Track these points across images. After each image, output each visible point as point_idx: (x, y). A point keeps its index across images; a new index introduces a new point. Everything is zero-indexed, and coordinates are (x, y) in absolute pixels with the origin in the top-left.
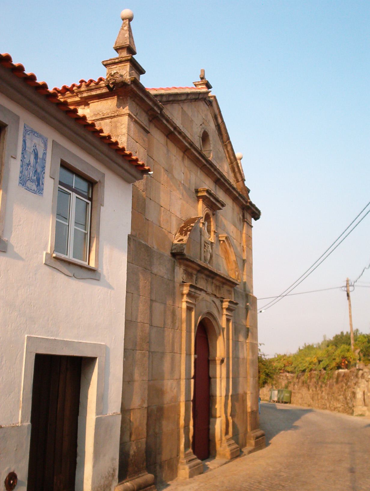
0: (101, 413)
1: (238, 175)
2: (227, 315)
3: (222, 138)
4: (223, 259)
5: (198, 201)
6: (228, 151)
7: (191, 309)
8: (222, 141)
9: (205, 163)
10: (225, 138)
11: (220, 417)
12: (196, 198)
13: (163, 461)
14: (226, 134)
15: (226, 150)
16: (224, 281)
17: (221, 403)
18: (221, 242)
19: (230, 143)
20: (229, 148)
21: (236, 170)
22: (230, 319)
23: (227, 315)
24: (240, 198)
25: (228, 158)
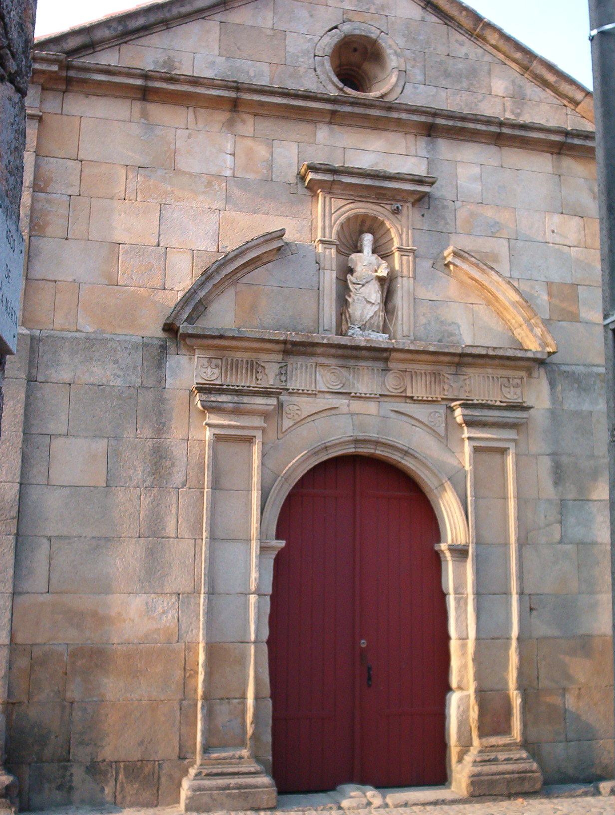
0: (496, 732)
1: (565, 88)
2: (469, 439)
3: (460, 26)
4: (475, 307)
5: (316, 196)
6: (495, 47)
7: (506, 451)
8: (464, 33)
9: (329, 107)
10: (468, 23)
11: (460, 688)
12: (308, 193)
13: (104, 761)
14: (464, 13)
15: (489, 48)
16: (457, 359)
17: (464, 653)
18: (452, 267)
19: (489, 25)
20: (493, 38)
21: (551, 78)
22: (508, 448)
23: (469, 439)
24: (569, 141)
25: (506, 62)
